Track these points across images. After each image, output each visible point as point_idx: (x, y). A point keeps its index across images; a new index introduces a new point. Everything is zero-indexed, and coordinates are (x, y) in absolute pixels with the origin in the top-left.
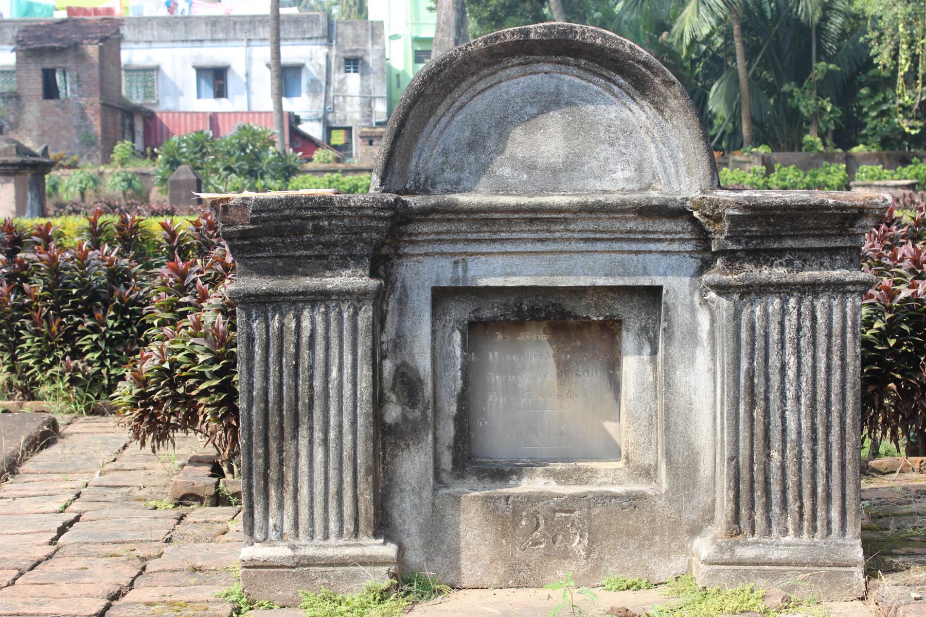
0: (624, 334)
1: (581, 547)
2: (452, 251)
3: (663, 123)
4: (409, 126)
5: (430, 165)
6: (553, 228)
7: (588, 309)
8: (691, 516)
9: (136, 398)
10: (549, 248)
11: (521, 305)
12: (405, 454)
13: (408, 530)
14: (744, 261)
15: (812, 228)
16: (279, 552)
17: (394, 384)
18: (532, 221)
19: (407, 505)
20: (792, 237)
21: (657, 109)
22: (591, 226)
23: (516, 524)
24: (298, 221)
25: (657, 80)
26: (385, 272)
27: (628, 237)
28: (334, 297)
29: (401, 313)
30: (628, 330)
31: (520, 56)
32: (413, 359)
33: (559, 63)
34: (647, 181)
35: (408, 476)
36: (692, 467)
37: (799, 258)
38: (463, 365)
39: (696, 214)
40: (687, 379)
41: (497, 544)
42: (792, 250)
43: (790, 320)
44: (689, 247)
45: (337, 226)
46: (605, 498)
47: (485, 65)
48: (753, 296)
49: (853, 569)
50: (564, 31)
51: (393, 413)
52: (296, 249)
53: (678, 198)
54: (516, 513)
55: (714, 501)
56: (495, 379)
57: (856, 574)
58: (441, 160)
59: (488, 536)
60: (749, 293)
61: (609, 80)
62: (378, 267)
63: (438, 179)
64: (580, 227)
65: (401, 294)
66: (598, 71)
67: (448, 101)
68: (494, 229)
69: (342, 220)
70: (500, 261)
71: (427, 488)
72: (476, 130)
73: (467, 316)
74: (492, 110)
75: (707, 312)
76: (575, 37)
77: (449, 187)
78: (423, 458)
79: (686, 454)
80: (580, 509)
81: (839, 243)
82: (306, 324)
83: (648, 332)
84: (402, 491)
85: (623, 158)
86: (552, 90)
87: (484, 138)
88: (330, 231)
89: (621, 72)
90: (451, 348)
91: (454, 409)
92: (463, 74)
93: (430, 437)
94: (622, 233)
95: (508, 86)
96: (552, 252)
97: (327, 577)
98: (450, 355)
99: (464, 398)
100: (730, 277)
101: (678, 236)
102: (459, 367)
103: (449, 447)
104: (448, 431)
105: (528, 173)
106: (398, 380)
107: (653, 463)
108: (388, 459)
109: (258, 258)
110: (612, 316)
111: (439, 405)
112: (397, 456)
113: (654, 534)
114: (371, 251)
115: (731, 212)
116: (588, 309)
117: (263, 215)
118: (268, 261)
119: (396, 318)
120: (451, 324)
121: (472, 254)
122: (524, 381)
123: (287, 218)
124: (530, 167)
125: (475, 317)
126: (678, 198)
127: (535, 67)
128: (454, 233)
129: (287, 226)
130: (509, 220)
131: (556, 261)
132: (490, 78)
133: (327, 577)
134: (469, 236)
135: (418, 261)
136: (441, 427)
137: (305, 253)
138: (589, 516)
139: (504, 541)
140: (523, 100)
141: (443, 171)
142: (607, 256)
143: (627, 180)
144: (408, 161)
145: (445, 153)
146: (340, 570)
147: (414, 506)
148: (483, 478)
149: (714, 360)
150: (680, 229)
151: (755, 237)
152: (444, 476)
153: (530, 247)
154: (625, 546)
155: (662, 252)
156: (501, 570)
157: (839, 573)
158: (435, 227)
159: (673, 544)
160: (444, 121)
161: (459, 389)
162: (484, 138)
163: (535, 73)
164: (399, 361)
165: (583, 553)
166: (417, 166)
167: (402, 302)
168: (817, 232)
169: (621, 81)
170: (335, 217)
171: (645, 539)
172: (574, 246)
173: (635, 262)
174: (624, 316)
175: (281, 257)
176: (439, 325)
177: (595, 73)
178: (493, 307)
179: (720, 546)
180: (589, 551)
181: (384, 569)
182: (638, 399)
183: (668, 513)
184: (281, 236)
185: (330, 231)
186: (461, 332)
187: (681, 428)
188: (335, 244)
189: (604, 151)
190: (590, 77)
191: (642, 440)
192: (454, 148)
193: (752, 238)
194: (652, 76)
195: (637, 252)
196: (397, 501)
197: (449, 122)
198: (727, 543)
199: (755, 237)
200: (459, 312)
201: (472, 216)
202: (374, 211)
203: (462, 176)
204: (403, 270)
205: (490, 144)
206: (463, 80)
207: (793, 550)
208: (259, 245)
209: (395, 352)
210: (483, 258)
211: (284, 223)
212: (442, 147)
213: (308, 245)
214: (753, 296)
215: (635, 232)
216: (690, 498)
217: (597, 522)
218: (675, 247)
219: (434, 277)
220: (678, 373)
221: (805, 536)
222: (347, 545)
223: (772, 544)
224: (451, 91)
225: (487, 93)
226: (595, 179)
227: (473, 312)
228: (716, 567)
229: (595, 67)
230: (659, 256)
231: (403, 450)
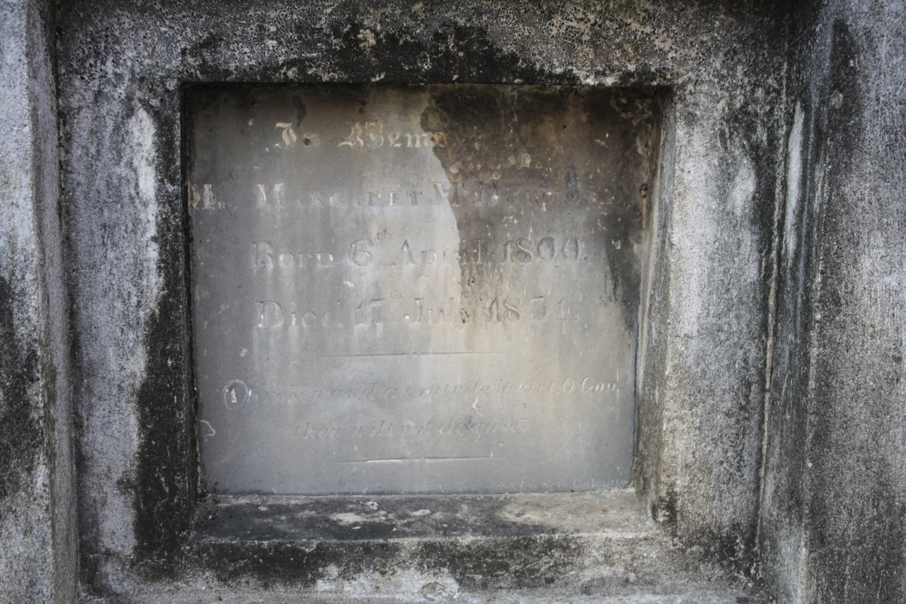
0: (681, 131)
7: (571, 50)
11: (356, 28)
30: (691, 120)
73: (176, 63)
79: (871, 513)
83: (750, 128)
90: (122, 170)
102: (152, 231)
103: (124, 485)
107: (744, 522)
110: (644, 73)
111: (90, 353)
116: (571, 50)
120: (121, 91)
125: (203, 67)
136: (96, 422)
148: (236, 574)
152: (111, 573)
161: (152, 304)
174: (686, 75)
182: (711, 332)
186: (156, 115)
187: (862, 436)
191: (718, 454)
220: (866, 263)
227: (197, 49)
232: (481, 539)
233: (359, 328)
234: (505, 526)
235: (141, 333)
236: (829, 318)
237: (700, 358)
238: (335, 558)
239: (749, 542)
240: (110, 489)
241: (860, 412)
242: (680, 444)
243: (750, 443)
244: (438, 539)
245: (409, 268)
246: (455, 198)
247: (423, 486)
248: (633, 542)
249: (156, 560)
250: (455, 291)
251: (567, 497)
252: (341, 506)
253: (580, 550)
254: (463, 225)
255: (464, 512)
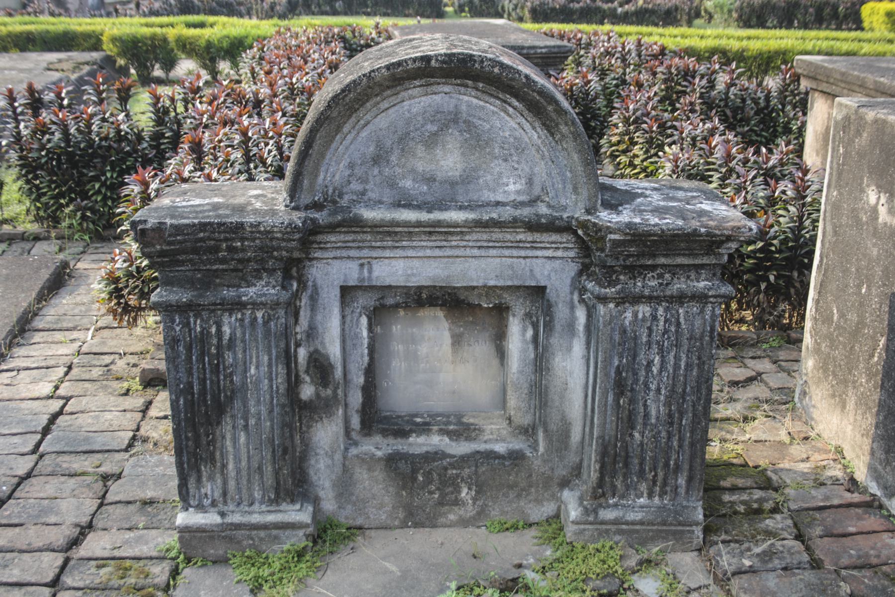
0: (511, 318)
1: (469, 497)
3: (553, 144)
4: (316, 147)
5: (337, 177)
6: (450, 238)
8: (561, 472)
9: (111, 294)
10: (446, 254)
12: (319, 425)
13: (323, 485)
14: (621, 274)
15: (684, 249)
16: (211, 519)
18: (430, 233)
19: (322, 465)
21: (549, 131)
22: (485, 237)
23: (415, 479)
24: (212, 242)
25: (550, 108)
26: (297, 272)
27: (518, 245)
28: (249, 307)
29: (313, 308)
30: (514, 315)
31: (421, 79)
32: (324, 347)
33: (458, 85)
34: (536, 194)
35: (322, 443)
36: (565, 433)
37: (669, 272)
38: (369, 344)
39: (580, 232)
40: (564, 364)
41: (398, 494)
42: (663, 266)
43: (657, 326)
44: (572, 254)
45: (250, 247)
46: (491, 455)
47: (388, 87)
48: (627, 305)
49: (694, 528)
50: (463, 59)
51: (307, 391)
52: (211, 264)
53: (565, 216)
54: (414, 471)
55: (582, 460)
56: (398, 347)
57: (696, 532)
58: (347, 172)
59: (391, 489)
60: (624, 303)
61: (505, 102)
62: (291, 269)
64: (475, 238)
66: (495, 93)
67: (353, 119)
68: (396, 238)
69: (254, 242)
70: (402, 264)
71: (339, 452)
72: (379, 145)
75: (584, 308)
77: (355, 198)
78: (334, 428)
79: (560, 424)
80: (469, 468)
81: (705, 260)
82: (227, 330)
83: (531, 317)
84: (317, 454)
85: (516, 173)
86: (451, 110)
87: (387, 152)
88: (243, 250)
89: (516, 96)
90: (358, 330)
91: (361, 380)
93: (341, 412)
94: (512, 242)
95: (410, 105)
96: (448, 257)
98: (357, 336)
99: (370, 371)
100: (608, 290)
101: (562, 246)
102: (366, 346)
103: (357, 411)
104: (356, 399)
105: (427, 185)
107: (531, 424)
108: (304, 429)
109: (178, 271)
110: (501, 304)
111: (349, 377)
112: (311, 426)
113: (530, 486)
114: (282, 266)
115: (613, 237)
118: (187, 273)
119: (309, 313)
120: (358, 310)
121: (376, 258)
122: (423, 349)
123: (202, 240)
124: (430, 180)
126: (565, 216)
127: (435, 88)
128: (359, 242)
130: (410, 232)
132: (393, 98)
133: (252, 539)
134: (374, 244)
135: (327, 264)
137: (221, 267)
138: (476, 472)
139: (404, 493)
140: (424, 118)
141: (349, 182)
142: (498, 260)
143: (518, 192)
144: (316, 176)
145: (351, 166)
146: (262, 534)
147: (328, 467)
148: (387, 435)
150: (565, 240)
151: (633, 256)
152: (354, 435)
153: (429, 252)
155: (548, 258)
156: (401, 515)
157: (682, 532)
158: (342, 237)
159: (546, 494)
160: (350, 137)
161: (366, 364)
162: (387, 152)
163: (435, 93)
164: (312, 349)
165: (470, 502)
166: (324, 180)
167: (314, 299)
168: (687, 252)
169: (516, 104)
170: (247, 239)
171: (522, 490)
172: (468, 252)
174: (512, 304)
175: (199, 270)
176: (348, 311)
177: (492, 95)
178: (396, 296)
179: (586, 509)
180: (475, 500)
181: (301, 533)
182: (521, 372)
183: (543, 470)
186: (368, 316)
187: (557, 404)
188: (249, 260)
189: (498, 166)
190: (487, 98)
191: (523, 405)
192: (359, 162)
193: (629, 256)
194: (545, 104)
195: (525, 258)
196: (313, 462)
197: (355, 139)
199: (633, 256)
200: (364, 301)
203: (367, 187)
204: (313, 271)
205: (393, 158)
206: (367, 101)
207: (646, 512)
208: (178, 261)
210: (387, 261)
211: (199, 244)
212: (348, 160)
213: (223, 261)
214: (627, 305)
215: (524, 242)
216: (562, 458)
217: (483, 478)
218: (559, 253)
219: (342, 277)
220: (557, 360)
221: (657, 498)
222: (269, 511)
223: (629, 506)
224: (356, 111)
225: (391, 111)
226: (489, 190)
227: (378, 300)
228: (582, 527)
230: (544, 260)
231: (317, 422)
232: (455, 427)
233: (422, 365)
234: (463, 424)
235: (363, 372)
236: (547, 374)
237: (518, 379)
238: (415, 432)
239: (533, 429)
240: (354, 412)
241: (556, 398)
242: (512, 402)
243: (533, 402)
244: (444, 427)
245: (437, 349)
246: (450, 329)
247: (440, 410)
248: (499, 429)
249: (366, 431)
250: (450, 355)
251: (483, 414)
252: (416, 416)
253: (483, 431)
254: (452, 337)
255: (452, 419)
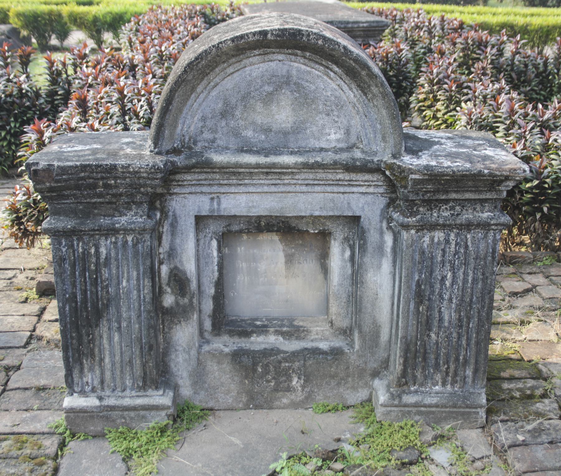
0: (332, 242)
1: (299, 384)
2: (209, 191)
3: (366, 102)
4: (175, 103)
5: (192, 128)
6: (283, 177)
7: (307, 225)
8: (373, 365)
9: (13, 221)
10: (280, 190)
11: (260, 222)
12: (178, 327)
13: (181, 375)
14: (420, 206)
15: (470, 187)
16: (91, 402)
17: (169, 281)
18: (267, 173)
19: (180, 359)
20: (457, 192)
21: (363, 91)
22: (311, 176)
23: (255, 370)
24: (91, 181)
25: (364, 73)
26: (160, 205)
27: (338, 183)
28: (121, 232)
29: (173, 233)
30: (335, 239)
31: (260, 49)
32: (182, 265)
33: (289, 54)
34: (353, 142)
35: (180, 341)
36: (376, 334)
37: (459, 205)
38: (219, 262)
39: (388, 173)
40: (375, 278)
41: (241, 382)
42: (454, 200)
43: (450, 248)
44: (381, 190)
45: (121, 184)
46: (316, 351)
47: (233, 56)
48: (425, 231)
49: (479, 410)
50: (294, 33)
51: (169, 300)
52: (91, 198)
53: (376, 159)
54: (255, 364)
55: (389, 356)
56: (242, 265)
57: (480, 413)
58: (200, 124)
59: (236, 378)
60: (423, 230)
61: (328, 68)
62: (155, 202)
63: (198, 139)
64: (303, 177)
65: (172, 220)
66: (319, 61)
67: (205, 82)
68: (239, 178)
69: (125, 180)
70: (245, 198)
71: (194, 349)
72: (226, 103)
73: (221, 229)
74: (239, 88)
75: (391, 234)
76: (302, 38)
77: (206, 145)
78: (190, 330)
79: (372, 327)
80: (299, 361)
81: (488, 196)
82: (103, 251)
83: (349, 241)
84: (176, 350)
85: (336, 125)
86: (284, 74)
87: (232, 108)
88: (116, 187)
89: (336, 63)
90: (210, 251)
91: (213, 291)
92: (216, 62)
93: (195, 316)
94: (333, 181)
95: (251, 70)
96: (282, 192)
97: (124, 418)
98: (209, 256)
99: (220, 284)
100: (410, 219)
101: (374, 183)
103: (209, 316)
104: (208, 306)
105: (265, 134)
106: (172, 279)
107: (349, 326)
108: (166, 330)
109: (64, 203)
110: (324, 230)
111: (202, 288)
112: (172, 328)
113: (348, 376)
114: (148, 199)
115: (413, 176)
116: (307, 225)
117: (64, 177)
118: (72, 205)
119: (169, 237)
121: (224, 193)
122: (262, 266)
123: (83, 178)
124: (267, 130)
125: (227, 230)
126: (376, 159)
127: (271, 57)
128: (210, 180)
129: (83, 184)
130: (251, 173)
131: (285, 198)
132: (237, 64)
133: (124, 418)
134: (222, 182)
135: (185, 198)
136: (203, 303)
137: (99, 200)
138: (304, 365)
139: (247, 381)
140: (262, 81)
141: (202, 132)
142: (322, 195)
143: (338, 141)
144: (175, 127)
145: (204, 119)
146: (132, 414)
147: (185, 360)
148: (233, 335)
149: (394, 266)
150: (375, 179)
151: (430, 192)
152: (206, 335)
153: (266, 189)
154: (328, 383)
155: (362, 193)
156: (244, 399)
157: (469, 413)
158: (196, 176)
159: (360, 383)
160: (202, 96)
162: (232, 108)
163: (271, 61)
164: (172, 266)
165: (300, 389)
166: (182, 130)
167: (174, 226)
168: (473, 189)
169: (336, 69)
170: (119, 178)
171: (341, 379)
172: (298, 188)
173: (342, 199)
174: (333, 230)
175: (81, 203)
176: (201, 235)
177: (317, 63)
178: (240, 223)
179: (392, 394)
180: (303, 387)
181: (163, 413)
182: (341, 285)
183: (357, 363)
184: (80, 190)
185: (116, 187)
186: (217, 240)
187: (369, 310)
188: (121, 195)
189: (321, 120)
190: (313, 65)
191: (342, 311)
192: (210, 116)
193: (426, 192)
194: (359, 69)
195: (343, 193)
196: (173, 357)
197: (206, 97)
198: (397, 392)
199: (430, 192)
200: (215, 227)
201: (223, 170)
202: (149, 174)
203: (216, 136)
204: (173, 203)
205: (238, 113)
206: (216, 66)
207: (441, 398)
208: (64, 195)
209: (169, 260)
210: (232, 195)
211: (80, 182)
212: (201, 115)
213: (100, 195)
214: (425, 231)
215: (343, 180)
216: (373, 354)
217: (310, 370)
218: (371, 190)
219: (197, 209)
220: (369, 275)
221: (449, 386)
222: (138, 396)
223: (427, 392)
224: (207, 75)
225: (235, 75)
226: (315, 139)
227: (226, 227)
228: (389, 409)
229: (317, 58)
230: (359, 195)
231: (176, 324)
232: (288, 329)
233: (261, 279)
234: (294, 326)
235: (214, 284)
236: (361, 286)
237: (338, 290)
238: (255, 332)
239: (350, 331)
240: (206, 317)
241: (369, 305)
242: (334, 309)
243: (350, 309)
244: (278, 329)
245: (273, 266)
246: (284, 250)
247: (276, 315)
248: (323, 331)
249: (216, 332)
250: (284, 271)
251: (310, 318)
252: (257, 320)
253: (310, 332)
254: (286, 256)
255: (285, 322)
